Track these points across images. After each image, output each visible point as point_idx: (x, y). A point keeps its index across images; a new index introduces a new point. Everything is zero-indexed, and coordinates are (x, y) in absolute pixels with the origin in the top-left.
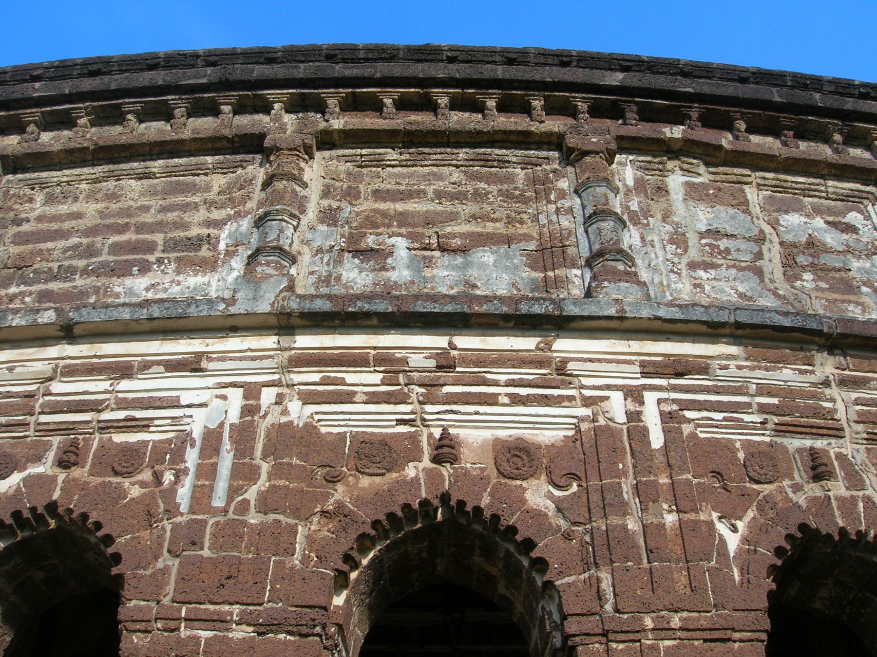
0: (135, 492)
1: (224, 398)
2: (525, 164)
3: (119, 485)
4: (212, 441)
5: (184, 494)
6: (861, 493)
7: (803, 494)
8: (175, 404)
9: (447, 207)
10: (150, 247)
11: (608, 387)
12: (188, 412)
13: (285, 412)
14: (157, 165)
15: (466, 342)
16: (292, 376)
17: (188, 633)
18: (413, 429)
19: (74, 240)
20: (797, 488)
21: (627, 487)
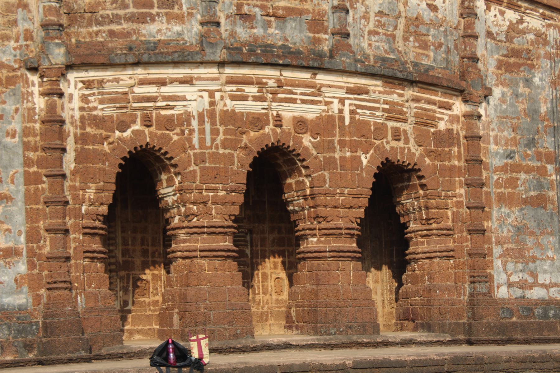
0: (175, 138)
1: (202, 97)
3: (169, 135)
4: (201, 116)
5: (195, 141)
6: (407, 146)
8: (184, 99)
11: (334, 97)
12: (189, 103)
13: (225, 105)
15: (288, 74)
16: (226, 87)
17: (206, 194)
18: (266, 111)
20: (388, 143)
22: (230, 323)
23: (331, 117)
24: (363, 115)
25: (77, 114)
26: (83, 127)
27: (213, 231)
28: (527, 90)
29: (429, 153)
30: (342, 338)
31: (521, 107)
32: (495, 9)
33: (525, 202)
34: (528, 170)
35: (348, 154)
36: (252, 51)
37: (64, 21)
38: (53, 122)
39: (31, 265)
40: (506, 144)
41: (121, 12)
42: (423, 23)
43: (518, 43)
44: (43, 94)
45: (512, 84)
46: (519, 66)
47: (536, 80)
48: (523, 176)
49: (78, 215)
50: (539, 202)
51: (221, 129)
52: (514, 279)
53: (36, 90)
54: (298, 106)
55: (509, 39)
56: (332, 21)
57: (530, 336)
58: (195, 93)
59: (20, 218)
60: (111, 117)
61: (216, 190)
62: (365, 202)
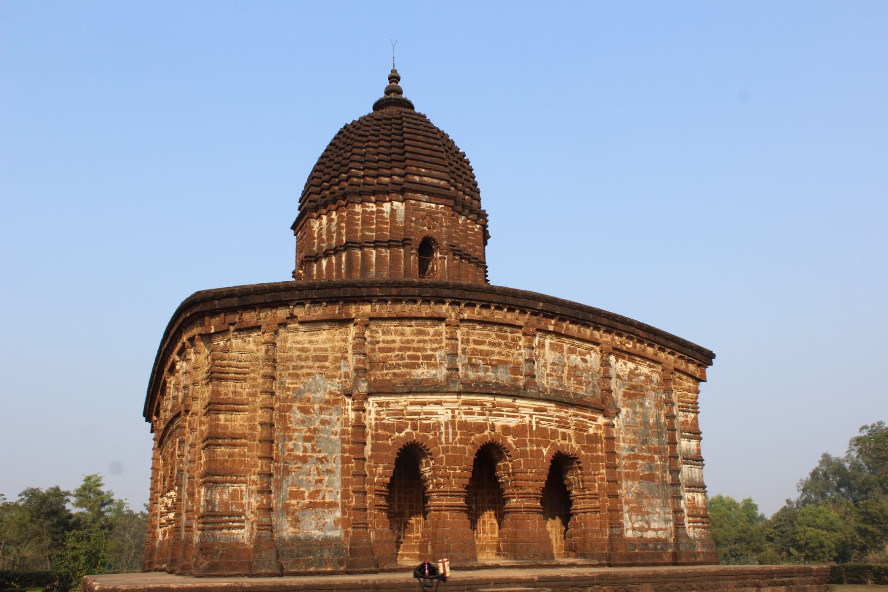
0: (431, 437)
2: (511, 333)
4: (446, 424)
5: (443, 439)
7: (560, 442)
8: (436, 414)
9: (491, 348)
10: (418, 358)
14: (413, 323)
15: (499, 399)
19: (397, 353)
21: (528, 439)
22: (463, 552)
23: (525, 426)
24: (544, 424)
25: (373, 422)
26: (376, 430)
27: (453, 494)
28: (642, 410)
29: (583, 448)
30: (531, 562)
31: (638, 420)
32: (621, 362)
33: (642, 478)
34: (643, 458)
35: (535, 448)
36: (477, 386)
37: (368, 367)
38: (360, 426)
39: (344, 513)
40: (630, 443)
41: (401, 362)
42: (579, 370)
43: (635, 381)
44: (353, 410)
45: (633, 406)
46: (636, 395)
47: (647, 404)
48: (640, 462)
49: (372, 482)
50: (650, 478)
51: (459, 432)
52: (636, 525)
53: (350, 407)
54: (505, 419)
55: (630, 379)
56: (524, 368)
57: (646, 561)
58: (443, 411)
59: (338, 484)
60: (393, 424)
61: (455, 469)
62: (546, 478)
